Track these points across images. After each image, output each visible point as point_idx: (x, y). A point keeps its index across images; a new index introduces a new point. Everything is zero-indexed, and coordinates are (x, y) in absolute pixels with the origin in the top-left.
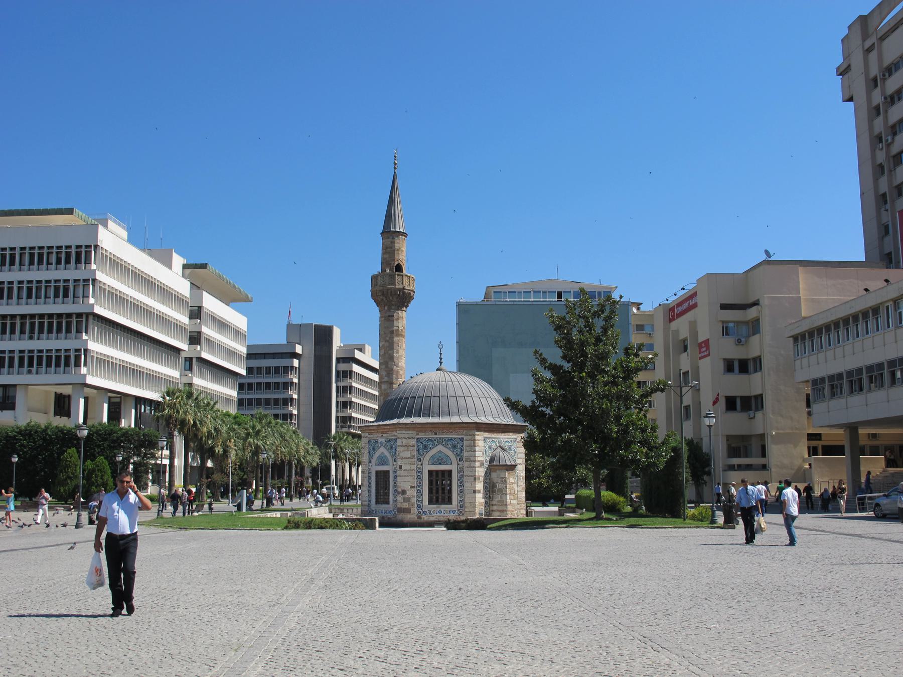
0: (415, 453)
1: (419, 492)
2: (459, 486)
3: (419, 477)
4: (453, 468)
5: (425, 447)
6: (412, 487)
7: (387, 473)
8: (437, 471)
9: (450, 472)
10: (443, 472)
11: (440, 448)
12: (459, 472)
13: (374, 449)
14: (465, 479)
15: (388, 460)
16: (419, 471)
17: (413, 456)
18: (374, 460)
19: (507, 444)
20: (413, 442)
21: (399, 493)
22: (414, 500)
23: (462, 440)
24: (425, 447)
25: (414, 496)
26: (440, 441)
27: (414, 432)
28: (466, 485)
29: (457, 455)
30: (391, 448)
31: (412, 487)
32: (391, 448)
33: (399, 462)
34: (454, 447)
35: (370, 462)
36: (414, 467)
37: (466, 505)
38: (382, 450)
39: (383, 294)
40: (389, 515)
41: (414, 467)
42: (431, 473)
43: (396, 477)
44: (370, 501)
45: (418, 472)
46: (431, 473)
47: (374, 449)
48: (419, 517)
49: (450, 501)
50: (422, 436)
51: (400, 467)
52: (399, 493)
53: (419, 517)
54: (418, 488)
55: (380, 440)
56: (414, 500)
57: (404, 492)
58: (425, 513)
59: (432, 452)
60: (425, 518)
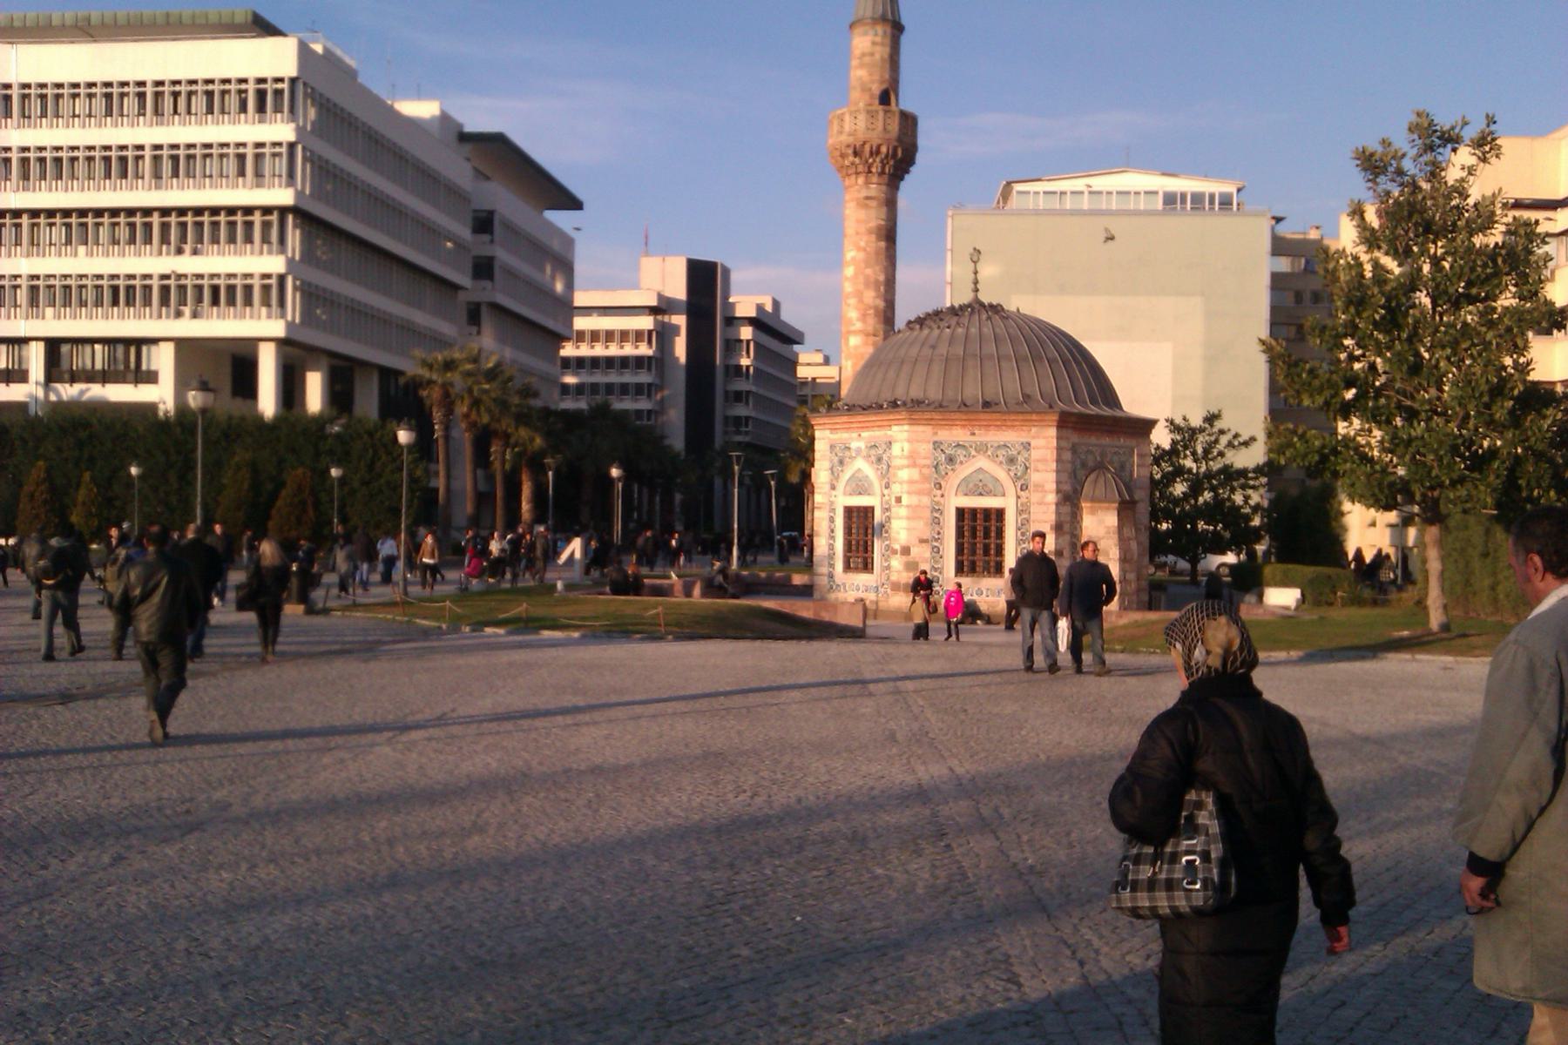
3: (936, 522)
4: (1008, 503)
5: (951, 460)
6: (922, 541)
7: (868, 511)
8: (974, 511)
9: (1000, 513)
10: (987, 512)
12: (1019, 512)
13: (841, 462)
15: (871, 484)
16: (937, 510)
17: (925, 479)
18: (841, 486)
20: (925, 448)
21: (895, 552)
23: (1027, 446)
24: (951, 460)
26: (982, 449)
27: (928, 429)
29: (1016, 478)
30: (879, 460)
31: (922, 541)
32: (879, 460)
33: (896, 489)
34: (1012, 461)
35: (833, 488)
36: (926, 500)
39: (856, 154)
41: (926, 500)
42: (961, 513)
45: (934, 510)
46: (961, 513)
47: (841, 462)
51: (899, 500)
52: (895, 552)
54: (934, 543)
55: (854, 445)
59: (965, 470)
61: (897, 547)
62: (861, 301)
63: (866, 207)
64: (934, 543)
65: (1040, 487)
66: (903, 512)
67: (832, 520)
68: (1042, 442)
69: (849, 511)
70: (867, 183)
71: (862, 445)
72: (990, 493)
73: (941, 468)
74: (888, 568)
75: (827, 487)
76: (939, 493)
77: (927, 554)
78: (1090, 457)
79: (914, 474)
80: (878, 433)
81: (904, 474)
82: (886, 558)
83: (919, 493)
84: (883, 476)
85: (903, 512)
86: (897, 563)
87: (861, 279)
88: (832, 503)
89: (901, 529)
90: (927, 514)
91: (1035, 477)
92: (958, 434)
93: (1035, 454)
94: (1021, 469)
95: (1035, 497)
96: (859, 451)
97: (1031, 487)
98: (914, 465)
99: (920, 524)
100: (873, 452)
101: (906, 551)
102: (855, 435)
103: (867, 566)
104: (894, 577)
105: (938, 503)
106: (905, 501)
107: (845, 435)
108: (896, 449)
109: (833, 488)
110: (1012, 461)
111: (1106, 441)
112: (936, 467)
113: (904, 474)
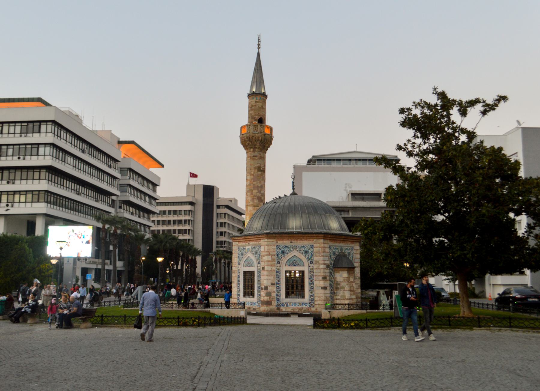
0: (275, 257)
1: (278, 288)
2: (310, 284)
3: (278, 276)
4: (306, 269)
5: (283, 252)
6: (272, 284)
7: (252, 273)
11: (295, 253)
12: (310, 272)
13: (242, 254)
14: (315, 278)
15: (253, 262)
16: (278, 272)
17: (273, 260)
18: (242, 263)
19: (346, 251)
21: (262, 289)
22: (274, 295)
23: (312, 246)
24: (283, 252)
25: (274, 292)
26: (295, 248)
27: (274, 240)
28: (316, 282)
29: (308, 259)
30: (256, 253)
31: (272, 284)
32: (256, 253)
33: (262, 264)
35: (239, 264)
36: (274, 268)
37: (316, 299)
38: (249, 254)
40: (254, 306)
41: (274, 268)
43: (260, 276)
44: (239, 295)
47: (242, 254)
48: (278, 309)
49: (303, 297)
50: (280, 242)
51: (263, 268)
52: (262, 289)
53: (278, 309)
54: (277, 285)
55: (247, 248)
56: (274, 295)
57: (266, 288)
58: (283, 305)
59: (289, 256)
60: (283, 309)
61: (263, 287)
62: (252, 194)
63: (254, 159)
64: (277, 285)
65: (317, 262)
66: (265, 273)
67: (239, 276)
68: (318, 245)
69: (245, 273)
70: (254, 151)
71: (250, 247)
72: (298, 265)
73: (280, 255)
74: (260, 295)
75: (237, 264)
76: (279, 265)
77: (275, 290)
78: (337, 251)
79: (269, 258)
80: (255, 243)
81: (265, 258)
82: (259, 291)
83: (271, 265)
84: (257, 259)
85: (265, 273)
86: (263, 293)
87: (252, 186)
88: (239, 270)
89: (264, 280)
90: (274, 273)
91: (315, 258)
92: (287, 242)
93: (315, 250)
94: (310, 255)
95: (315, 266)
96: (248, 250)
97: (314, 263)
98: (269, 255)
99: (271, 278)
100: (254, 250)
101: (266, 288)
102: (247, 244)
103: (252, 294)
104: (262, 299)
105: (278, 269)
106: (266, 268)
107: (244, 244)
108: (262, 249)
109: (239, 264)
110: (306, 252)
111: (342, 244)
112: (277, 255)
113: (265, 258)
